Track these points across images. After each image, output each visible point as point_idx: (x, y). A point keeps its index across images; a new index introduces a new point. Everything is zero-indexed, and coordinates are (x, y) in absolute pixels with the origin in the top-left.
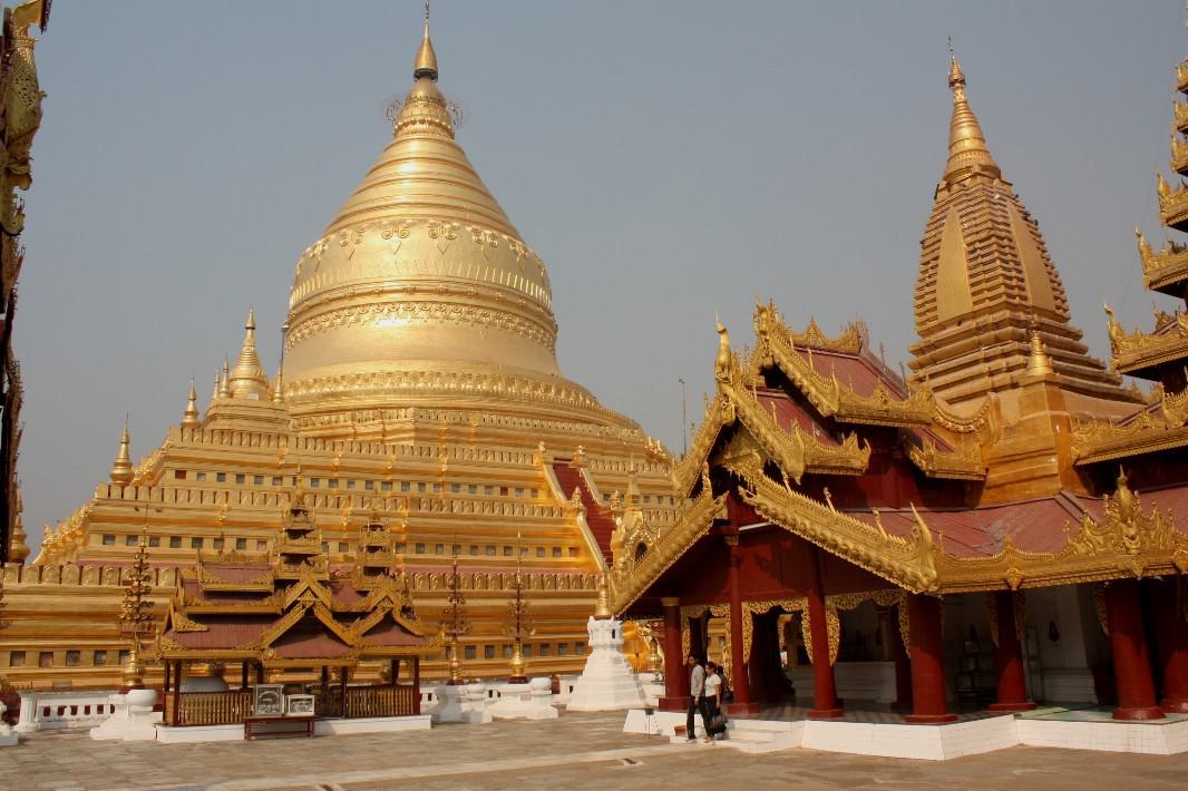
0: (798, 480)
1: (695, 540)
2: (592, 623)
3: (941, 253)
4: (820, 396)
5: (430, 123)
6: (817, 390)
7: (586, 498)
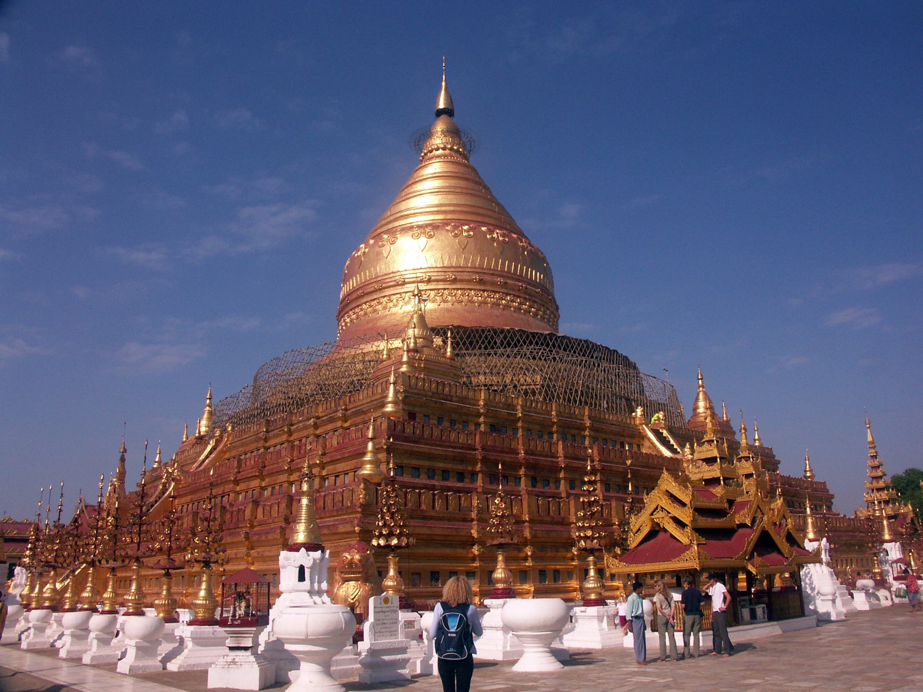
5: (451, 149)
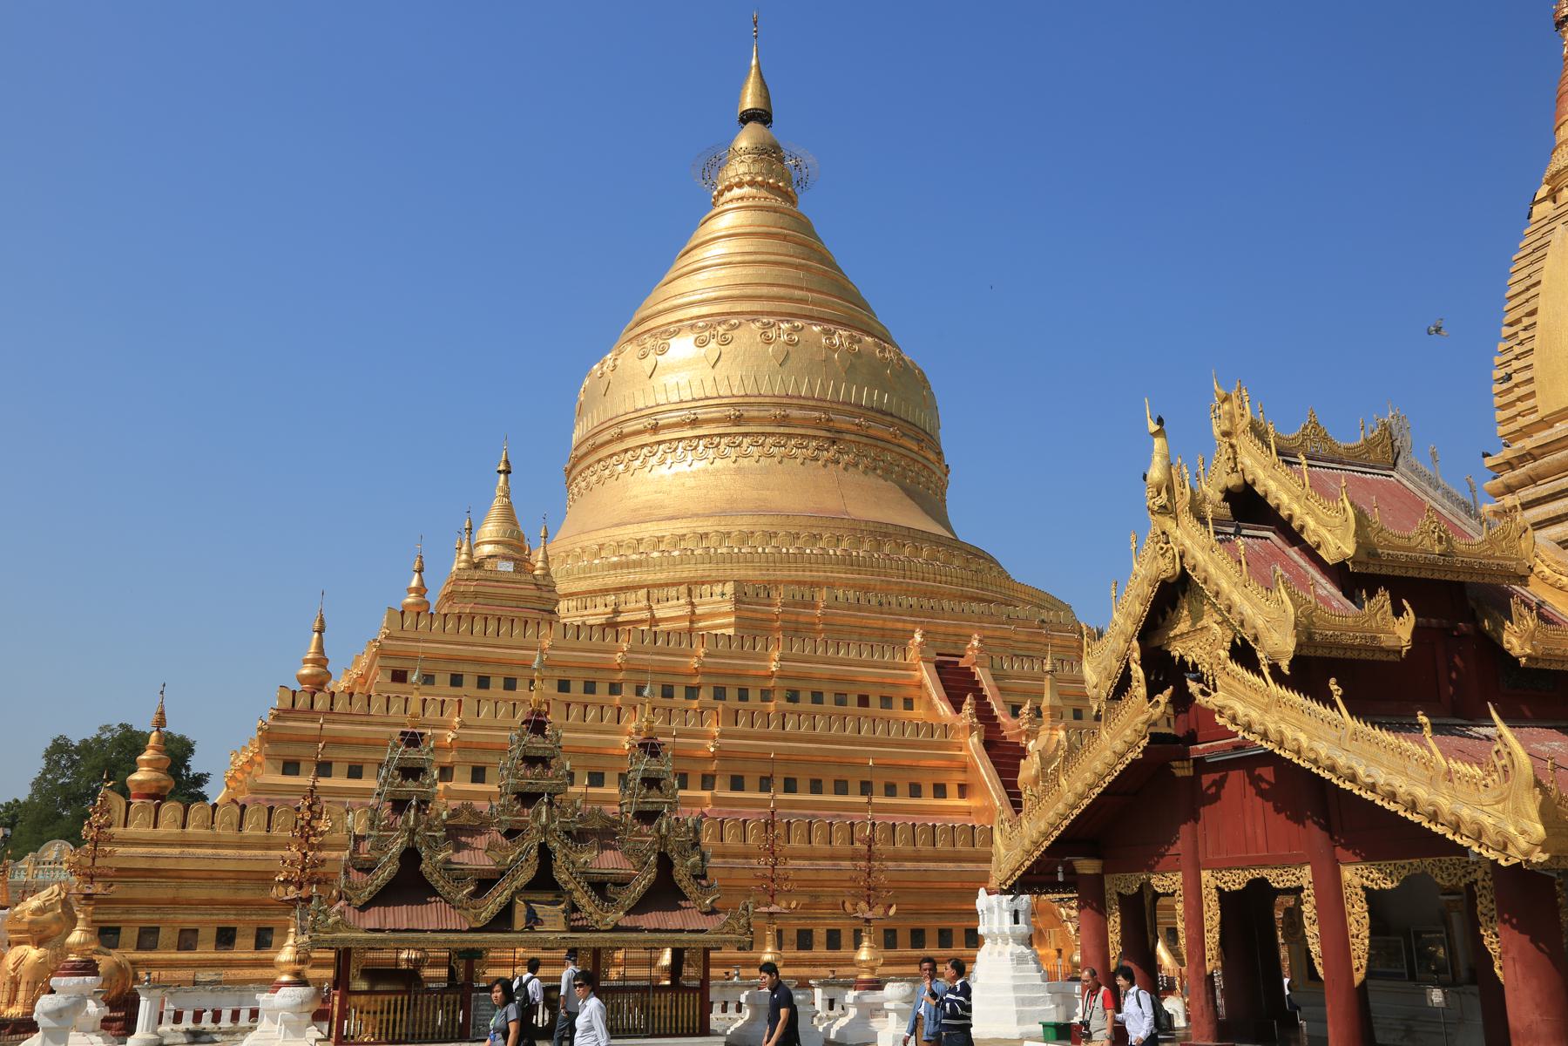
0: (1285, 666)
1: (1120, 767)
2: (983, 901)
3: (1540, 303)
4: (1323, 532)
5: (761, 185)
6: (1318, 520)
7: (984, 713)
